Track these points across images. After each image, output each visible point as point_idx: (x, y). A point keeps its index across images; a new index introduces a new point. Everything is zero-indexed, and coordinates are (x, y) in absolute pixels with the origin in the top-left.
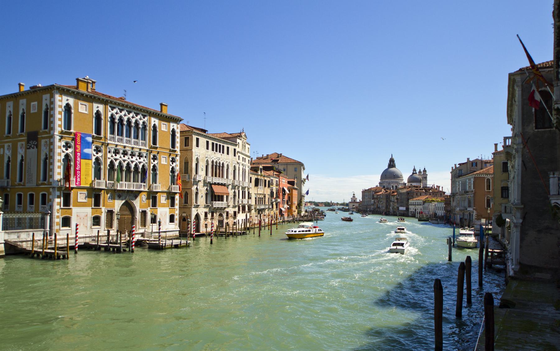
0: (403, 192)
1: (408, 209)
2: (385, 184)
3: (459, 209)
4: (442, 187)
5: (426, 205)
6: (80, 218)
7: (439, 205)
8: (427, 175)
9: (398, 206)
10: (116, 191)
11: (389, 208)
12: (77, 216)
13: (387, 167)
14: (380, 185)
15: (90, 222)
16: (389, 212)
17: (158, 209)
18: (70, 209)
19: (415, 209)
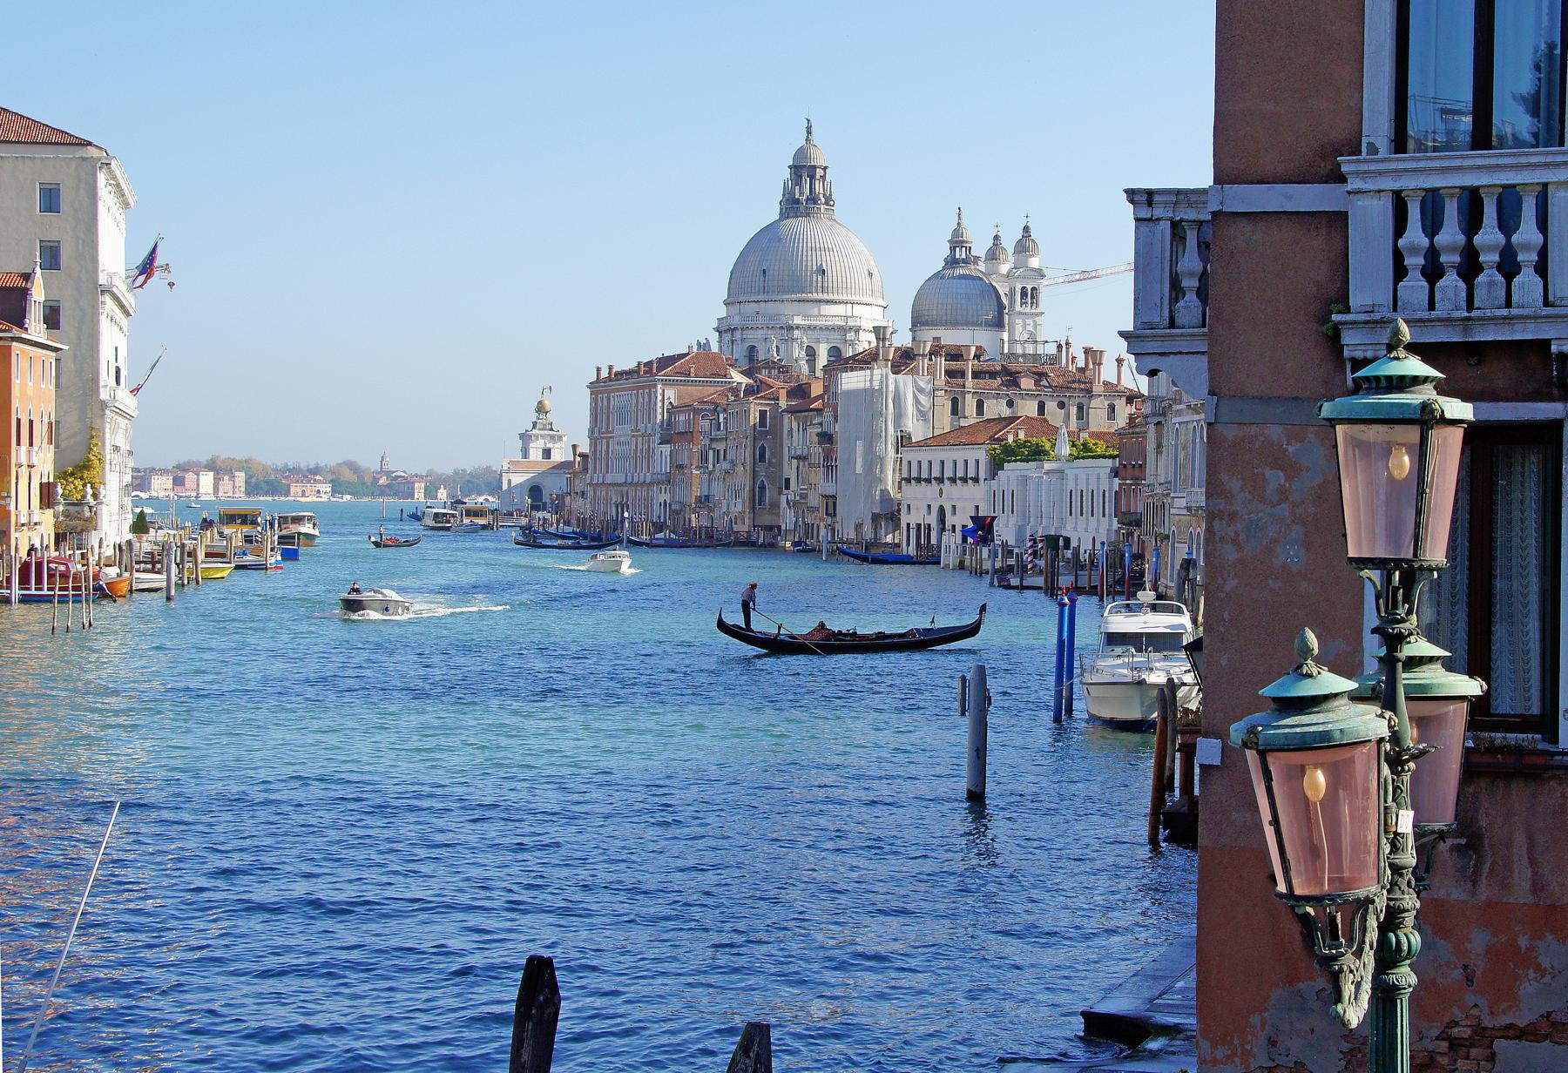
2: (760, 334)
3: (1182, 503)
7: (1082, 477)
9: (830, 491)
11: (775, 505)
13: (771, 212)
14: (720, 342)
19: (942, 509)
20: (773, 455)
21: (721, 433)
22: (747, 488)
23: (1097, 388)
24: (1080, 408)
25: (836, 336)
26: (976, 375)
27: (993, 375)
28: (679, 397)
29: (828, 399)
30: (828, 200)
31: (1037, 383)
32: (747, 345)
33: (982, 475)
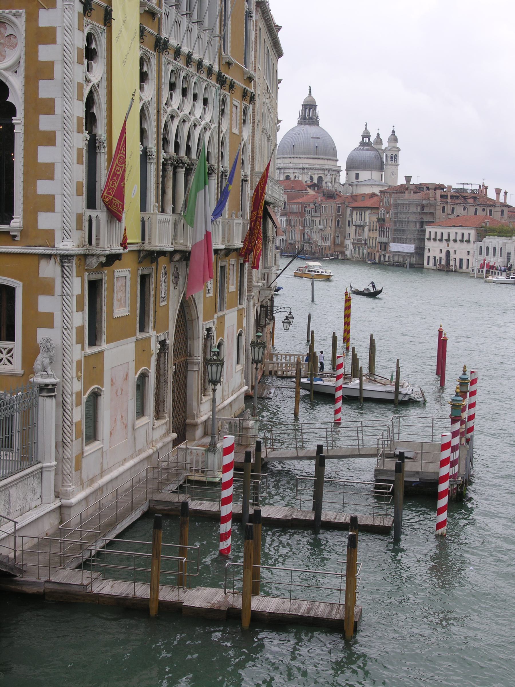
0: (406, 202)
1: (420, 251)
2: (291, 171)
4: (506, 193)
5: (491, 241)
6: (116, 393)
8: (399, 150)
9: (384, 240)
10: (177, 257)
11: (342, 243)
12: (112, 383)
15: (132, 405)
16: (343, 253)
17: (226, 316)
18: (101, 353)
19: (448, 253)
20: (342, 224)
21: (316, 214)
22: (332, 236)
23: (497, 204)
24: (491, 211)
25: (321, 172)
26: (452, 197)
27: (457, 197)
28: (288, 198)
29: (383, 204)
30: (317, 117)
31: (474, 200)
32: (286, 175)
33: (472, 239)
